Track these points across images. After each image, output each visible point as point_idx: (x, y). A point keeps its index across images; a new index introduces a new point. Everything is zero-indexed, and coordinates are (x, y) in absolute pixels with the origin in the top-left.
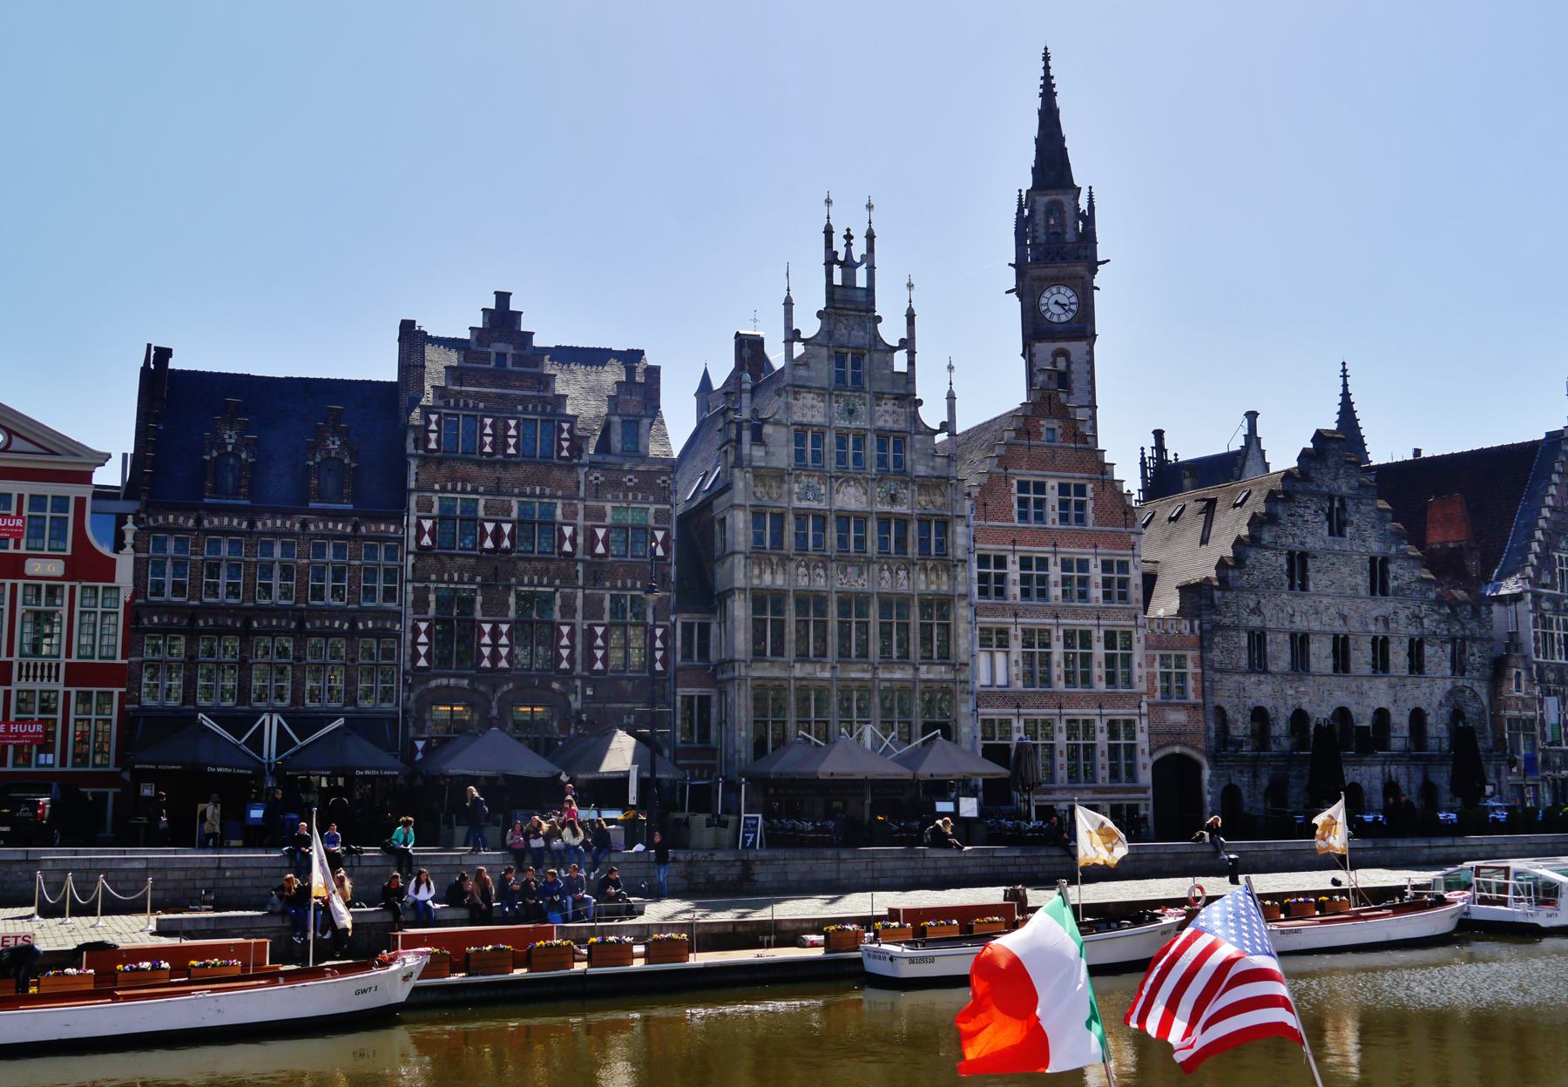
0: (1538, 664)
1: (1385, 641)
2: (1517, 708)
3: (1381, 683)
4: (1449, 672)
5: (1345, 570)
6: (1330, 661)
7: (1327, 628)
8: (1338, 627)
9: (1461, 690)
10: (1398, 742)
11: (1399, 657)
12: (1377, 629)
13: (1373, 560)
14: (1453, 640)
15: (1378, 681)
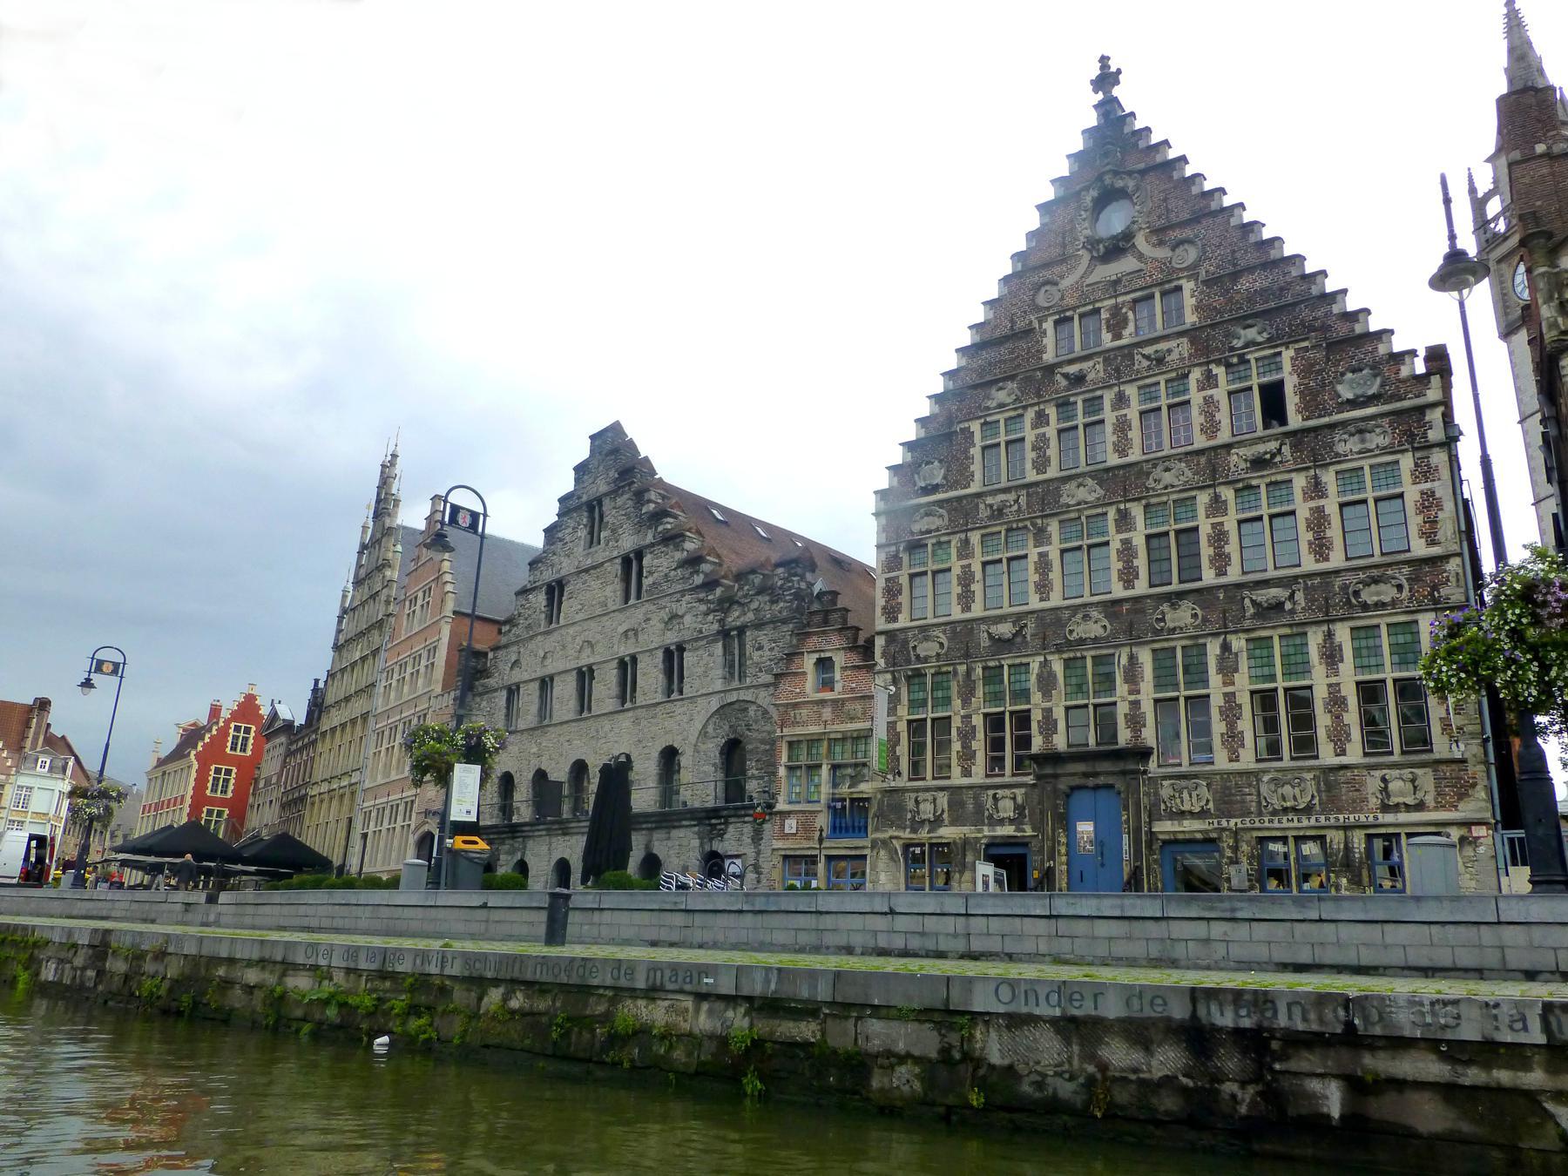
0: (890, 635)
1: (634, 659)
2: (818, 719)
3: (625, 721)
4: (719, 685)
5: (595, 584)
6: (573, 703)
7: (574, 665)
8: (584, 661)
9: (741, 706)
10: (644, 798)
11: (650, 676)
12: (625, 650)
13: (626, 562)
14: (724, 634)
15: (621, 717)
